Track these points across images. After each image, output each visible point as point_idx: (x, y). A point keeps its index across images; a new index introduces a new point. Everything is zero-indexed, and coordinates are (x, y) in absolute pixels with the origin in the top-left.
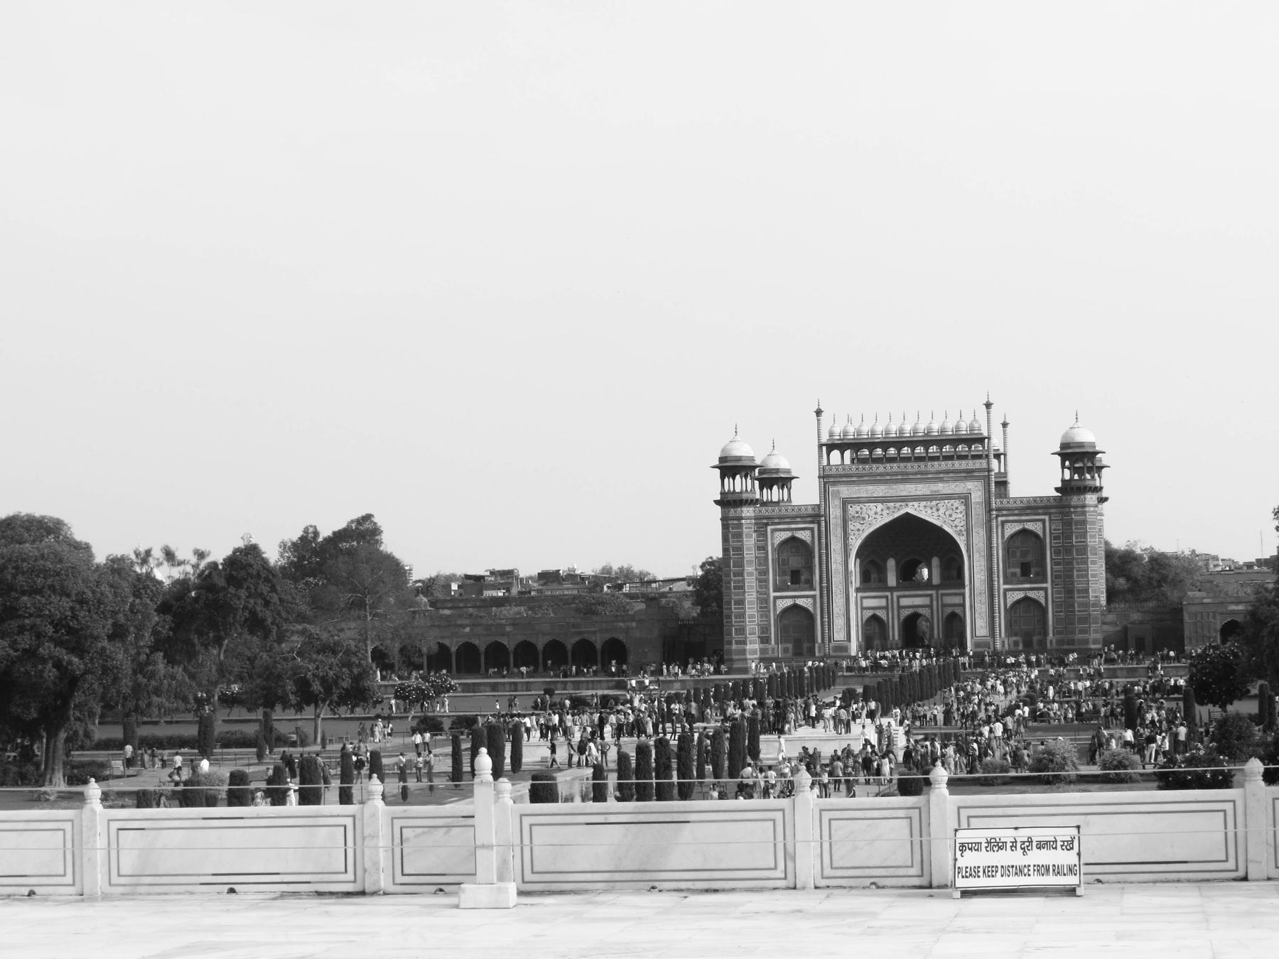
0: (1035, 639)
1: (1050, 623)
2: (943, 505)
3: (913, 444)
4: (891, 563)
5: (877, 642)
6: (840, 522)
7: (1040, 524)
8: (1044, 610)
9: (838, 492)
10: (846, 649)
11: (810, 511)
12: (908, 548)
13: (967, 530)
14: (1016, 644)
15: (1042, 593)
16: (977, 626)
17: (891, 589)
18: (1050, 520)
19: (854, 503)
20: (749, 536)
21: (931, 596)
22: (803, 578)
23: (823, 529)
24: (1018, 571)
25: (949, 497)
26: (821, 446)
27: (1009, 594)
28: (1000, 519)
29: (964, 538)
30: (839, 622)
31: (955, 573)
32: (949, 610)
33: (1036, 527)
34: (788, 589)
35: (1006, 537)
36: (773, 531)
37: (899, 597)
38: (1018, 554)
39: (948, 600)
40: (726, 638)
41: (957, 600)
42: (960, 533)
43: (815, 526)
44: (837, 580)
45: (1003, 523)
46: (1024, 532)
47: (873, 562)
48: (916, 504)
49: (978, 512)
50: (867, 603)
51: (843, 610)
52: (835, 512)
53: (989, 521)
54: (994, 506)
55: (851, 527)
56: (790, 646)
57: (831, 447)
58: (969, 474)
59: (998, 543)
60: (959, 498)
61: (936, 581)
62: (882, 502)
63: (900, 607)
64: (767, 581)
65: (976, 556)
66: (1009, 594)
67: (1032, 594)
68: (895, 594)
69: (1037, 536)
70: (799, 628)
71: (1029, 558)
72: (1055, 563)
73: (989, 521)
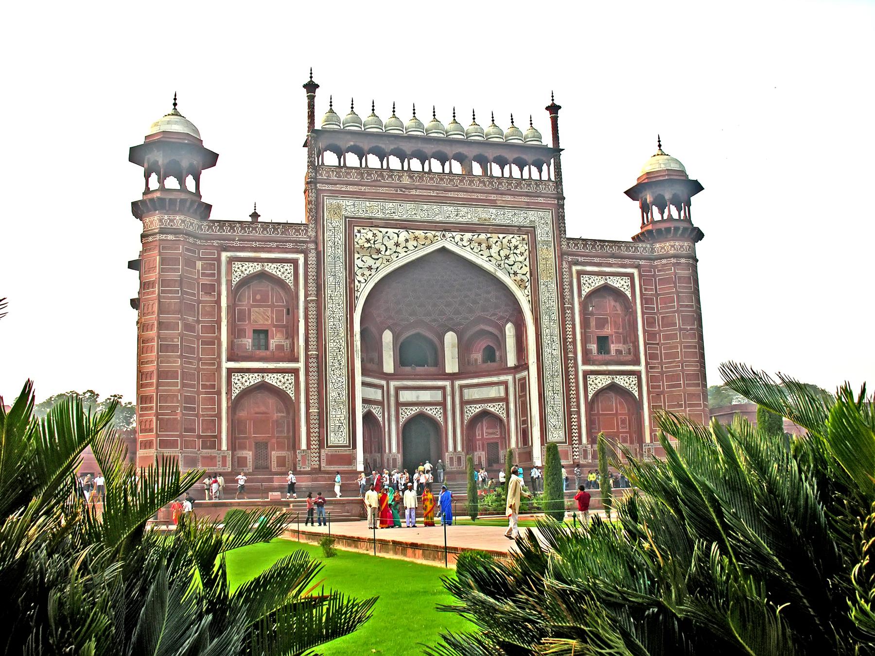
6: (340, 252)
9: (339, 207)
17: (388, 377)
19: (364, 227)
21: (443, 388)
22: (273, 343)
24: (594, 347)
25: (505, 229)
28: (575, 268)
30: (337, 416)
31: (477, 356)
32: (476, 409)
35: (584, 293)
42: (521, 284)
43: (301, 258)
44: (335, 345)
45: (580, 273)
46: (606, 290)
48: (458, 237)
49: (547, 255)
51: (345, 393)
54: (564, 247)
55: (358, 262)
56: (249, 454)
62: (406, 228)
63: (398, 404)
67: (621, 381)
68: (393, 384)
71: (608, 331)
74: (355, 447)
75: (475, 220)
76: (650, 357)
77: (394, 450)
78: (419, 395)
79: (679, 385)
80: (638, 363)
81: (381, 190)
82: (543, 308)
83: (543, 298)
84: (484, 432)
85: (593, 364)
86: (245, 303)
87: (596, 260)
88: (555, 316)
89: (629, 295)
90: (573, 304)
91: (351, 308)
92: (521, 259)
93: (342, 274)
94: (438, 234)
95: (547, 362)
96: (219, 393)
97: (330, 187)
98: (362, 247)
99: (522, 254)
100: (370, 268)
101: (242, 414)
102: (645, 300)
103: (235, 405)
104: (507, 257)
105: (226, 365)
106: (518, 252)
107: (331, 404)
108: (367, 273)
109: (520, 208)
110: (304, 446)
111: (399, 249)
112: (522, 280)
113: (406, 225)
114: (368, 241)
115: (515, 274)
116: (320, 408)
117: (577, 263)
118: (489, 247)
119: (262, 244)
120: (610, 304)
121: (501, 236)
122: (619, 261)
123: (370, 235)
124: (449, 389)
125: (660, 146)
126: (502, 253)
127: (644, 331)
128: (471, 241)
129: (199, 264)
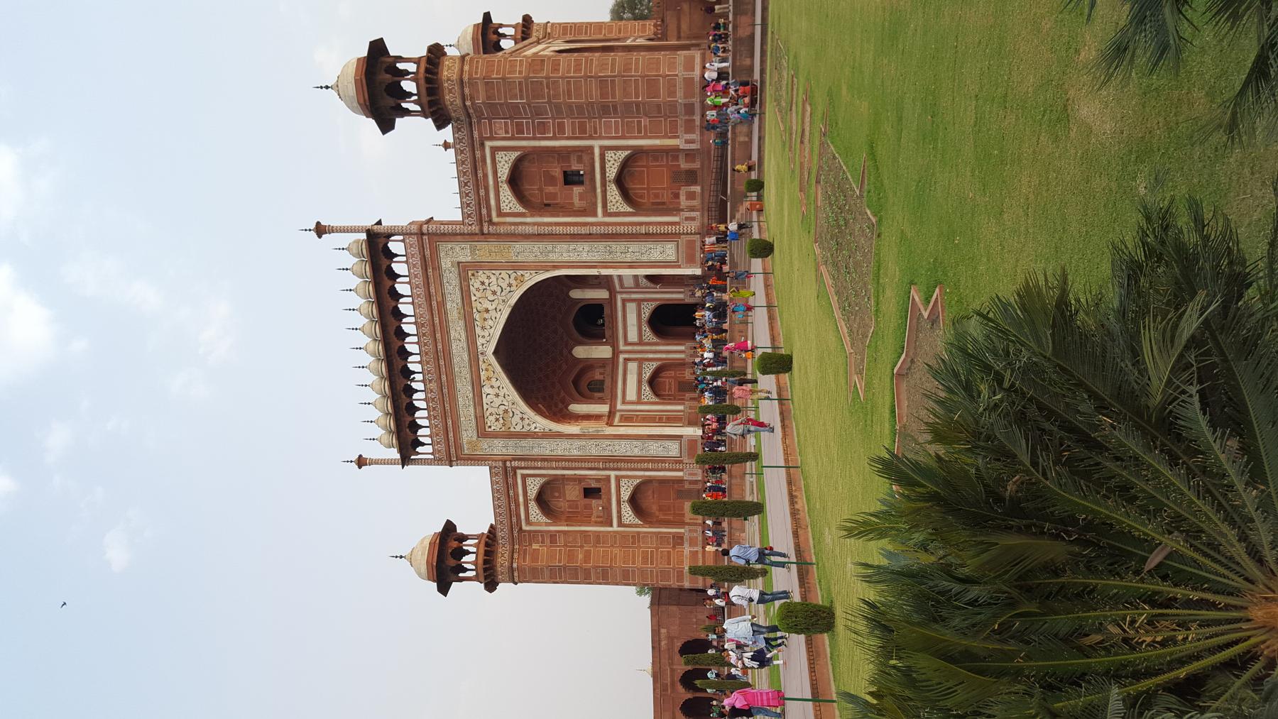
0: (684, 165)
1: (657, 142)
2: (480, 301)
4: (581, 352)
6: (511, 442)
7: (499, 155)
11: (500, 478)
12: (551, 344)
13: (515, 269)
14: (691, 196)
15: (609, 155)
18: (492, 138)
19: (485, 424)
20: (535, 557)
21: (624, 301)
22: (594, 485)
23: (523, 464)
24: (577, 190)
26: (405, 460)
27: (611, 208)
28: (495, 219)
29: (527, 276)
30: (654, 449)
33: (504, 165)
34: (607, 509)
35: (521, 210)
36: (528, 522)
37: (627, 343)
38: (551, 189)
43: (519, 472)
44: (593, 449)
45: (500, 214)
46: (515, 180)
47: (576, 383)
48: (480, 341)
49: (486, 251)
51: (635, 443)
52: (499, 447)
53: (498, 235)
54: (475, 229)
55: (518, 429)
59: (533, 222)
60: (467, 279)
64: (597, 534)
65: (553, 257)
66: (611, 208)
67: (612, 172)
68: (622, 347)
71: (557, 172)
72: (559, 133)
73: (498, 235)
74: (681, 436)
75: (462, 323)
76: (582, 133)
77: (682, 348)
78: (631, 322)
79: (615, 107)
80: (591, 148)
81: (448, 407)
82: (541, 259)
83: (532, 258)
85: (595, 204)
87: (482, 192)
88: (549, 248)
89: (517, 154)
90: (534, 224)
91: (560, 435)
92: (493, 279)
93: (530, 442)
94: (481, 358)
95: (596, 257)
96: (639, 533)
97: (453, 451)
98: (504, 425)
99: (488, 277)
100: (522, 419)
101: (654, 508)
102: (519, 132)
104: (494, 293)
105: (615, 528)
106: (487, 282)
107: (644, 453)
108: (527, 421)
109: (441, 276)
110: (680, 474)
111: (501, 394)
112: (516, 279)
113: (477, 386)
114: (497, 420)
115: (510, 285)
116: (648, 461)
117: (489, 215)
118: (487, 311)
119: (512, 500)
120: (531, 169)
121: (473, 298)
122: (479, 165)
123: (492, 418)
124: (624, 296)
125: (327, 87)
126: (491, 298)
127: (554, 138)
128: (483, 328)
129: (535, 546)
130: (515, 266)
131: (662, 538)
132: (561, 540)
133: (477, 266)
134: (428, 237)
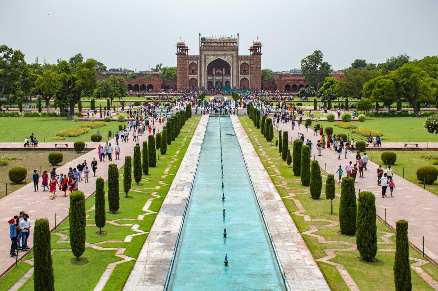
3: (220, 43)
4: (214, 69)
5: (210, 87)
8: (248, 81)
10: (204, 88)
16: (233, 84)
17: (214, 75)
25: (229, 55)
30: (203, 82)
31: (228, 72)
33: (247, 62)
39: (226, 78)
40: (177, 85)
41: (229, 78)
42: (231, 63)
44: (203, 73)
46: (245, 63)
47: (210, 69)
49: (235, 58)
50: (209, 78)
52: (203, 57)
57: (202, 43)
58: (233, 50)
61: (224, 73)
67: (246, 77)
69: (247, 64)
70: (193, 82)
71: (245, 69)
72: (251, 70)
76: (251, 73)
84: (228, 84)
86: (191, 67)
103: (190, 81)
113: (214, 55)
130: (233, 62)
131: (186, 83)
132: (185, 66)
133: (233, 57)
134: (237, 50)
